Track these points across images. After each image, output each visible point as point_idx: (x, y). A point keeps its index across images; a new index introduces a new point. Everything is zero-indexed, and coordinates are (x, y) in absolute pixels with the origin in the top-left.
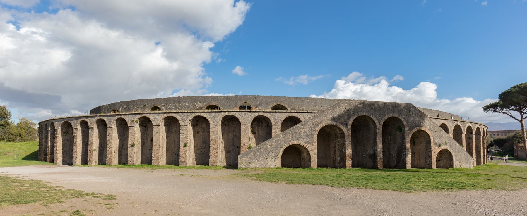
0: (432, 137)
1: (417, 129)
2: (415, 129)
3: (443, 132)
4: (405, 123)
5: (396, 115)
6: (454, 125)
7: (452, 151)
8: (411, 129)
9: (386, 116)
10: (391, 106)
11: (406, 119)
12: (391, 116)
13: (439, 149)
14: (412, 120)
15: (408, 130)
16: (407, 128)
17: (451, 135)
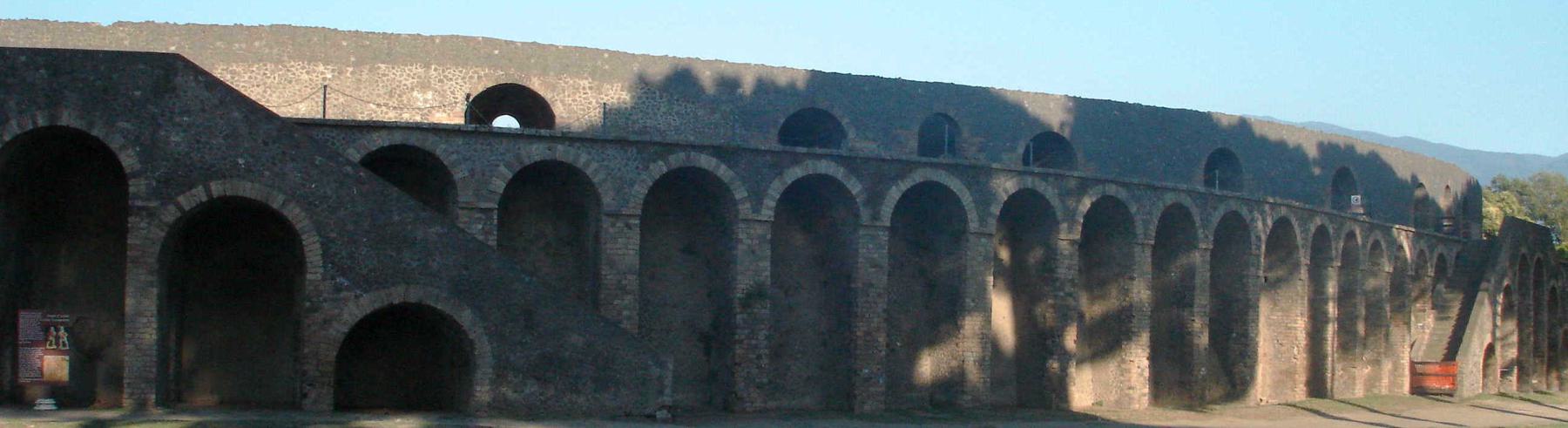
0: (317, 238)
1: (208, 191)
2: (194, 191)
3: (401, 208)
4: (128, 160)
5: (68, 119)
6: (659, 168)
7: (465, 317)
8: (167, 188)
9: (14, 123)
10: (42, 71)
11: (137, 137)
12: (41, 122)
13: (356, 308)
14: (178, 144)
15: (148, 200)
16: (143, 188)
17: (479, 228)
